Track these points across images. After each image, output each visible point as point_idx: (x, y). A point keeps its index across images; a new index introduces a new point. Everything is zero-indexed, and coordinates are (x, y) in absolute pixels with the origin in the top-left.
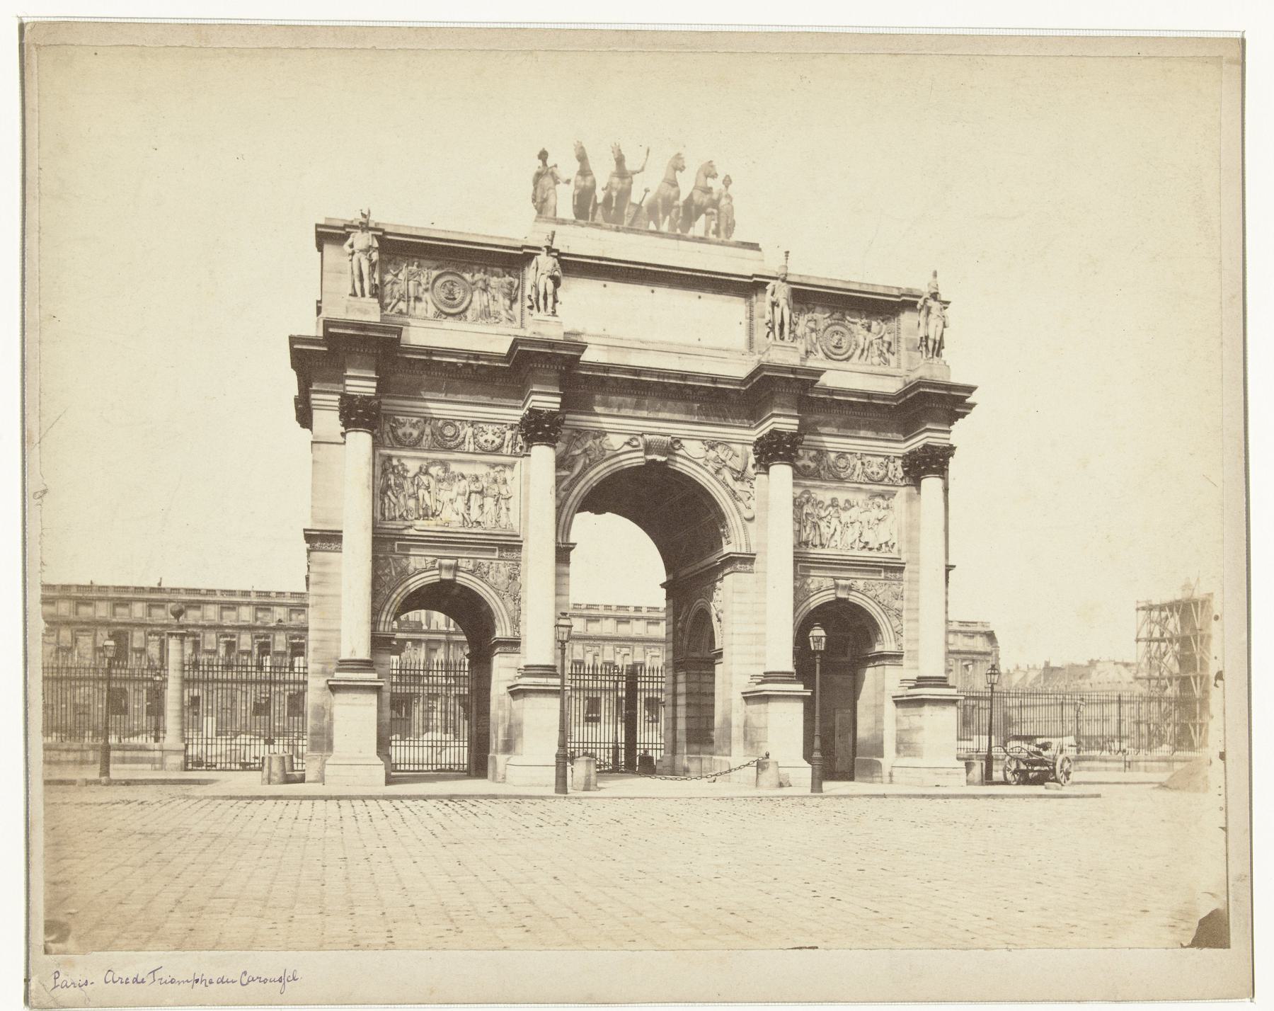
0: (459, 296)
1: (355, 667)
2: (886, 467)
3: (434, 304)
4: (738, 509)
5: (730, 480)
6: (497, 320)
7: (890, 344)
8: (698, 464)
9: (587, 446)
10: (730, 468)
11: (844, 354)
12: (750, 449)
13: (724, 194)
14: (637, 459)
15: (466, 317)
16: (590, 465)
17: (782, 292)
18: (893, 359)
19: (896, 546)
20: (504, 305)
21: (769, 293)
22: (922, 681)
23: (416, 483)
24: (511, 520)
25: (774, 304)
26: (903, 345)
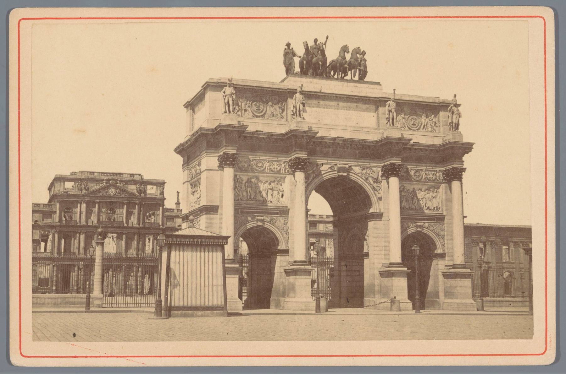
0: (261, 109)
1: (230, 262)
2: (436, 175)
3: (252, 112)
4: (375, 194)
5: (372, 183)
6: (277, 118)
7: (435, 122)
8: (359, 176)
9: (314, 169)
10: (372, 177)
11: (416, 127)
12: (380, 169)
13: (363, 58)
14: (335, 174)
15: (264, 117)
16: (315, 177)
17: (393, 105)
18: (437, 129)
19: (441, 208)
20: (279, 112)
21: (387, 106)
22: (455, 266)
23: (247, 185)
24: (284, 202)
25: (390, 111)
26: (441, 124)
